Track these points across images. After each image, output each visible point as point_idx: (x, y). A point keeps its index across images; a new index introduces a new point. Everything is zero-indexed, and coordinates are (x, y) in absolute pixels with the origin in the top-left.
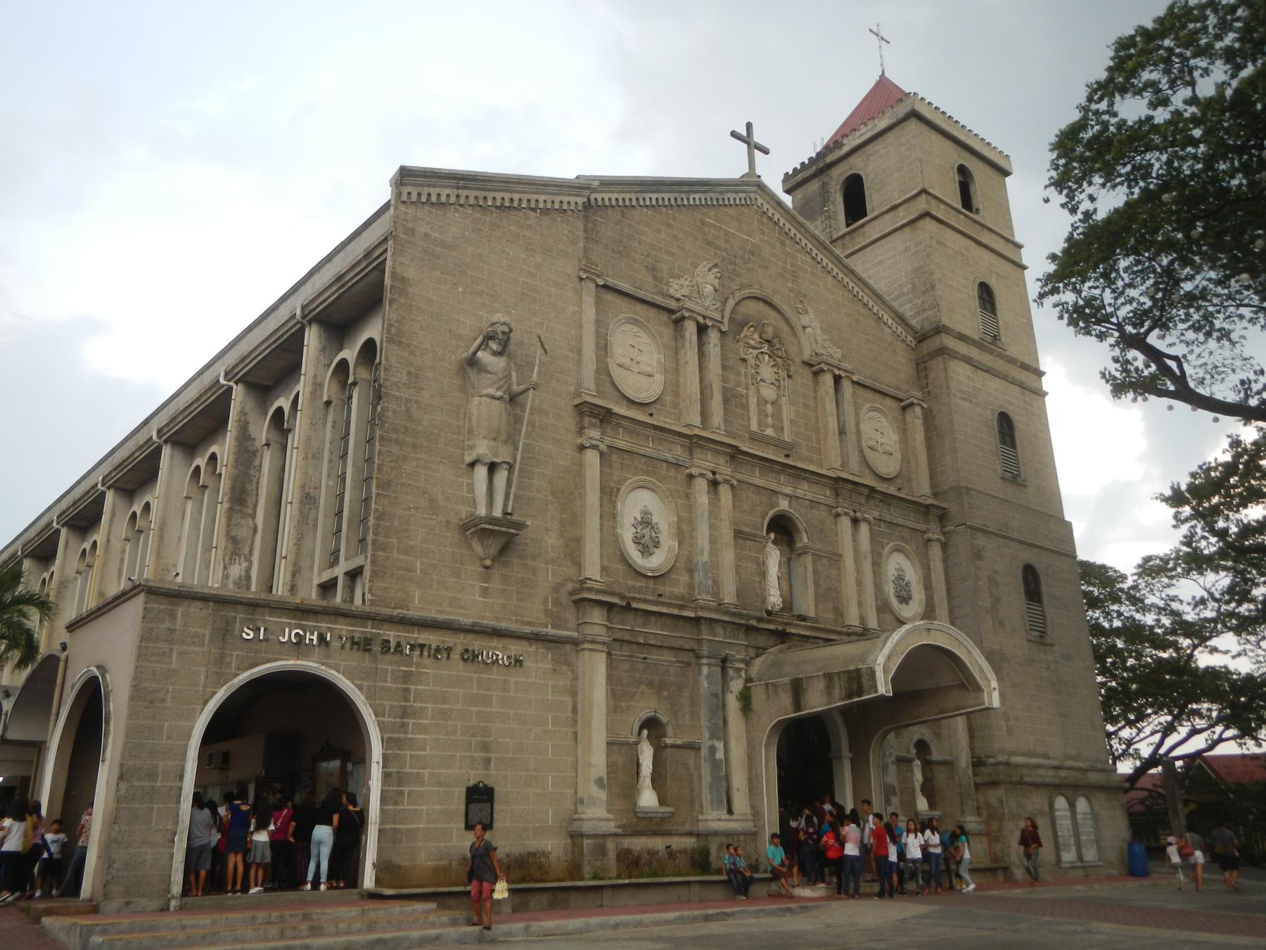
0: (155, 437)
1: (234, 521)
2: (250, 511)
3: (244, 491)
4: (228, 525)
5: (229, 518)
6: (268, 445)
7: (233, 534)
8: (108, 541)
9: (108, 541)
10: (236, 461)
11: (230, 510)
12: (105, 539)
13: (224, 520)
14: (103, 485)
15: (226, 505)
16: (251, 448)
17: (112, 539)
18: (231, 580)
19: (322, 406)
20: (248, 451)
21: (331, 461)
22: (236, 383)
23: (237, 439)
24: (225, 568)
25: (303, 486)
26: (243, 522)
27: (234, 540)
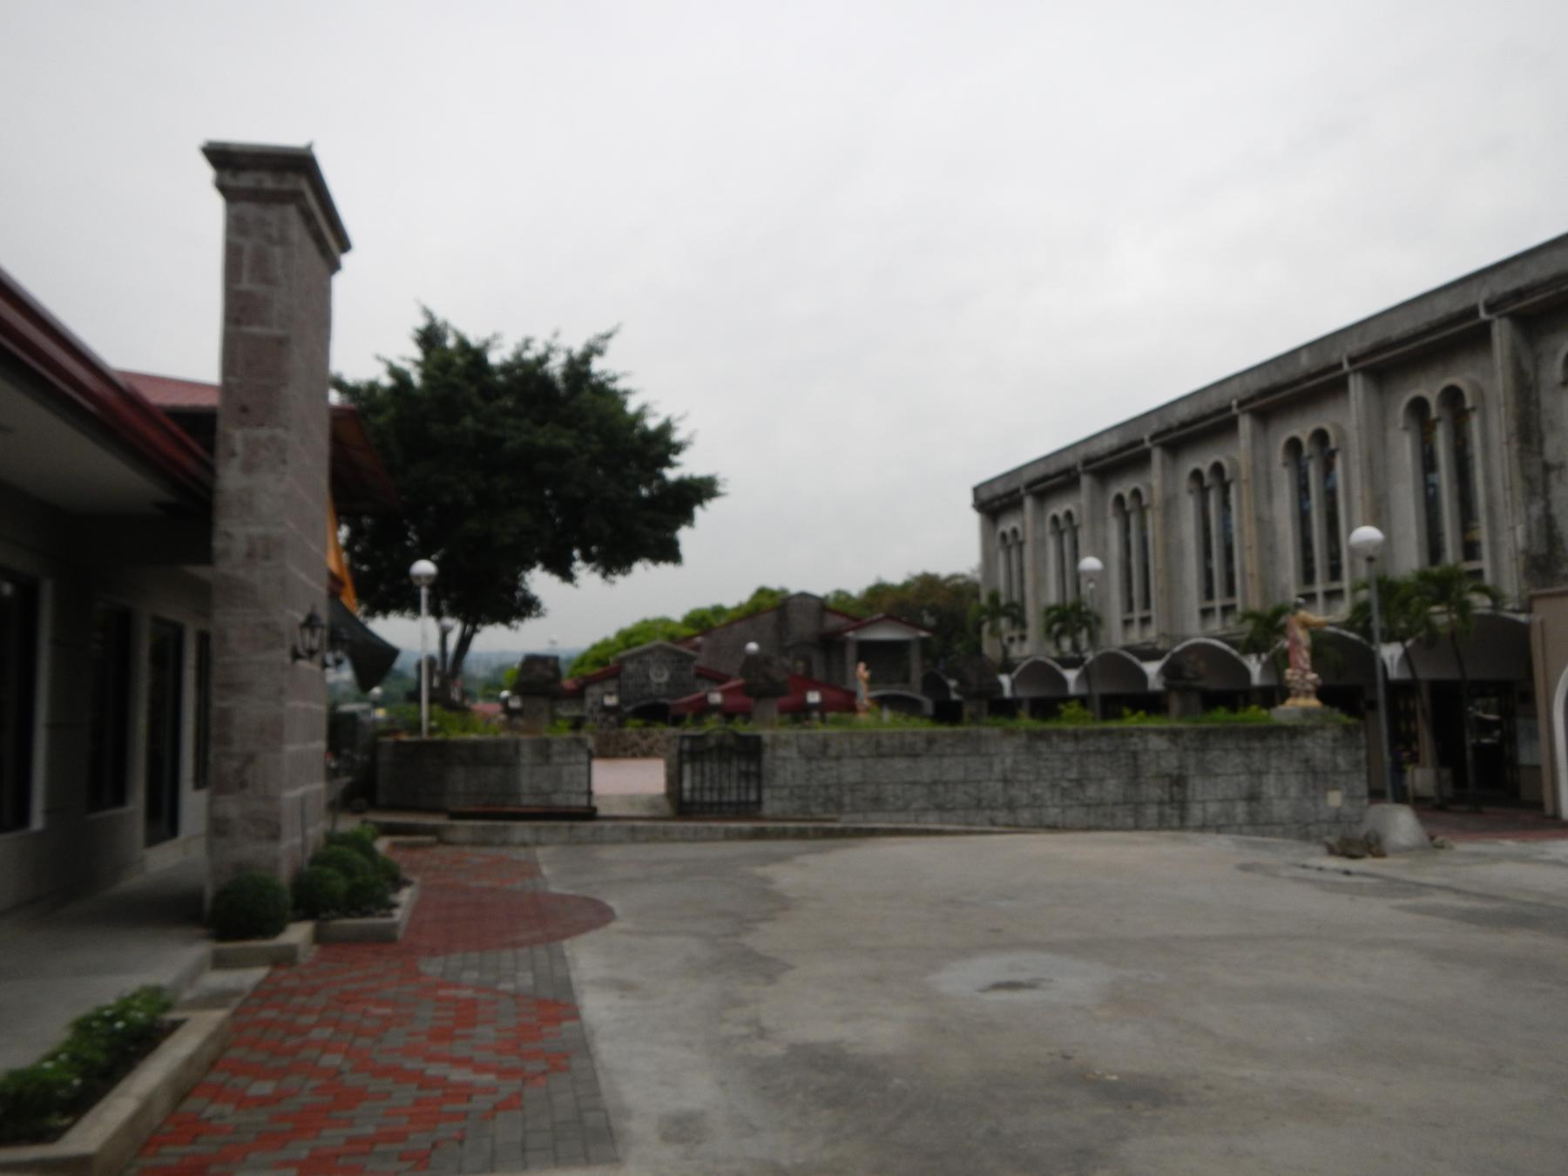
5: (1521, 458)
11: (1521, 450)
15: (1515, 446)
27: (1528, 480)
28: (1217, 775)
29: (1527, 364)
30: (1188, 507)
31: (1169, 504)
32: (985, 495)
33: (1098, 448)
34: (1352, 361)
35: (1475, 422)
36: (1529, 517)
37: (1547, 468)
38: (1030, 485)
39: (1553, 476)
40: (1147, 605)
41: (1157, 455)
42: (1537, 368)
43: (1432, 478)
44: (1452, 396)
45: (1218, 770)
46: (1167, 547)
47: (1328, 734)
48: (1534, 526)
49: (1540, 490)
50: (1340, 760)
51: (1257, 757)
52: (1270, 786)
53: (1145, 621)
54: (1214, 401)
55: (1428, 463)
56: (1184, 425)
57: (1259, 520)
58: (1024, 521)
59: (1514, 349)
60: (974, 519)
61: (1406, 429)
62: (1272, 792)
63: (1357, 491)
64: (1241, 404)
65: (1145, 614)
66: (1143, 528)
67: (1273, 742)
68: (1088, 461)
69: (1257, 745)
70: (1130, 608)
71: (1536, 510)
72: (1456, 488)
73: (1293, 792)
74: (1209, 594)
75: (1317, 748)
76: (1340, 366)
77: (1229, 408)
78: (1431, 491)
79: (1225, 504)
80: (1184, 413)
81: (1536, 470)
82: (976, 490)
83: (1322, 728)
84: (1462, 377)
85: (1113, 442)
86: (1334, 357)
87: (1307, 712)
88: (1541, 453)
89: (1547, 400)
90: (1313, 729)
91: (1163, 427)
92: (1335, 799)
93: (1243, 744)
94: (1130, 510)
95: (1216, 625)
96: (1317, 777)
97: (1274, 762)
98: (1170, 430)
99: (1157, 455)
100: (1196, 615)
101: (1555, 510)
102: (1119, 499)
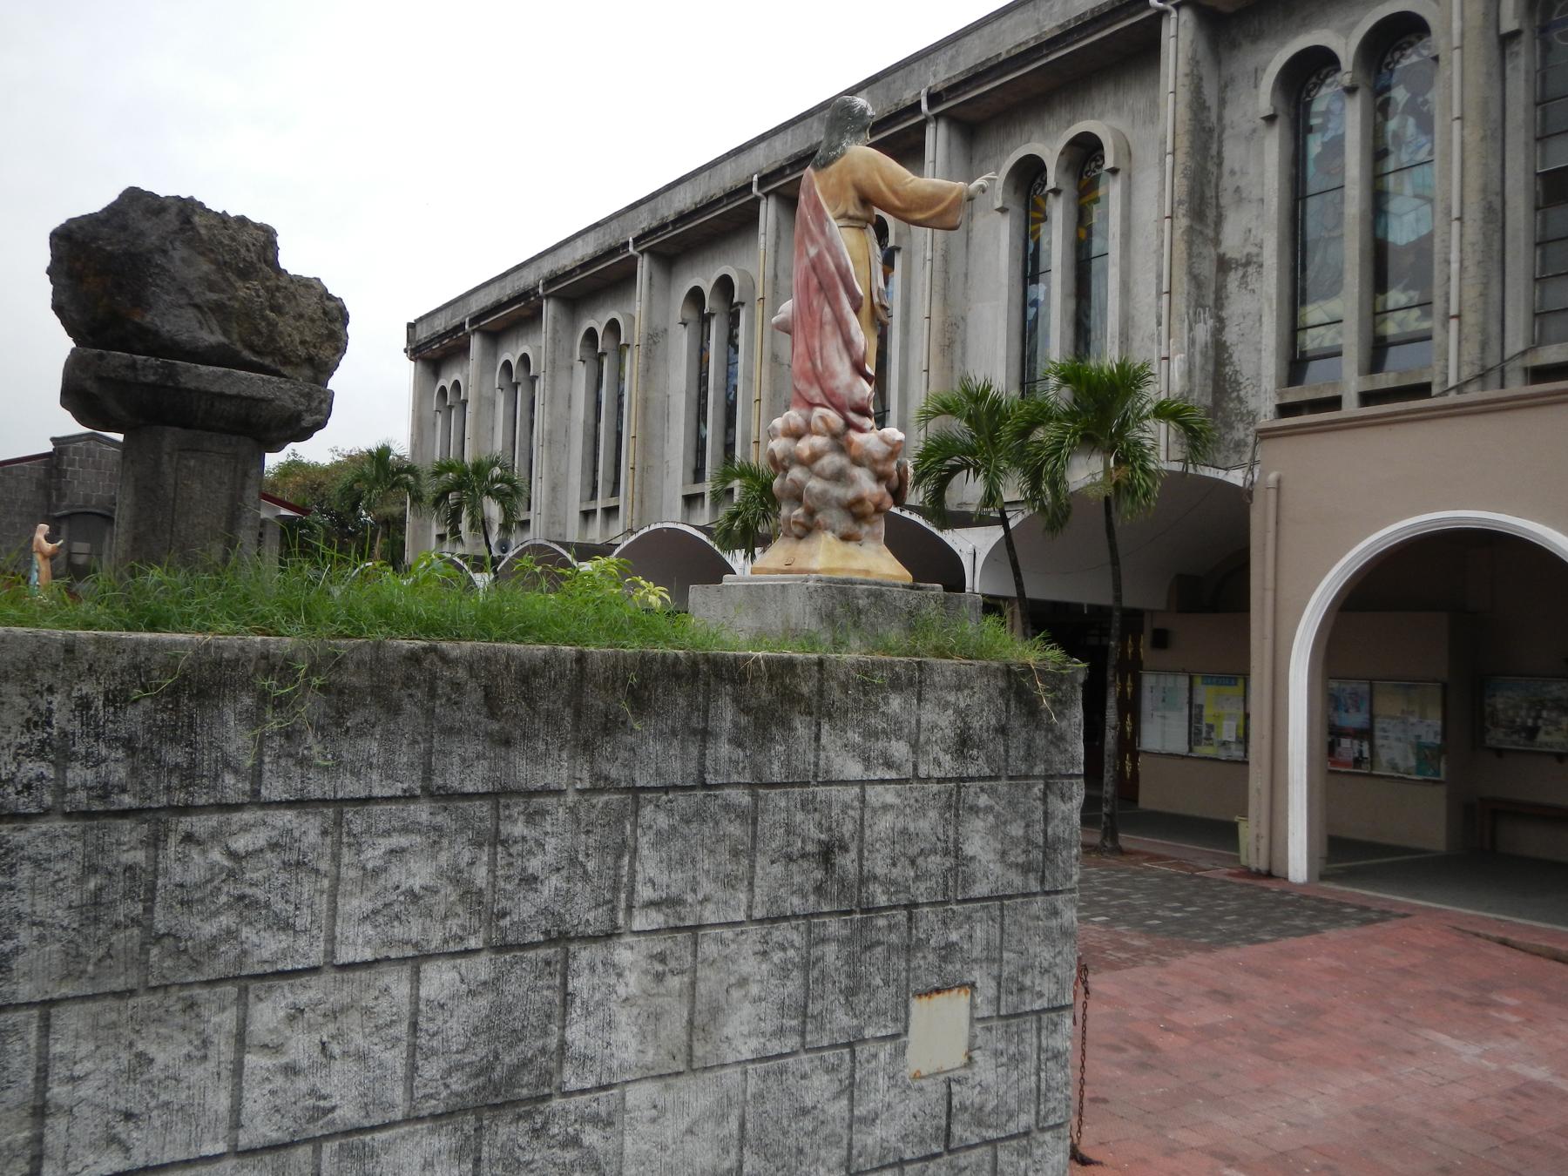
0: (924, 107)
1: (1195, 250)
2: (1210, 233)
3: (1202, 197)
4: (1190, 256)
5: (1190, 244)
6: (1270, 119)
7: (1196, 271)
8: (776, 276)
9: (776, 276)
10: (1192, 143)
11: (1190, 230)
12: (770, 273)
13: (1181, 247)
14: (760, 187)
15: (1183, 222)
16: (1207, 125)
17: (780, 274)
18: (1198, 348)
19: (1495, 40)
20: (1203, 129)
21: (1527, 144)
22: (1177, 7)
23: (1190, 106)
24: (1191, 329)
25: (1484, 190)
26: (1205, 251)
27: (1196, 280)
28: (250, 982)
29: (1210, 93)
30: (681, 343)
31: (655, 338)
32: (423, 334)
33: (568, 259)
34: (934, 99)
35: (1113, 190)
36: (1192, 342)
37: (1224, 265)
38: (476, 319)
39: (1233, 279)
40: (615, 491)
41: (644, 266)
42: (1222, 103)
43: (1038, 291)
44: (1085, 151)
45: (267, 946)
46: (645, 403)
47: (938, 719)
48: (1198, 359)
49: (1210, 300)
50: (978, 844)
51: (547, 843)
52: (617, 1012)
53: (610, 512)
54: (728, 178)
55: (1030, 269)
56: (683, 218)
57: (775, 358)
58: (469, 373)
59: (1194, 62)
60: (406, 371)
61: (1003, 210)
62: (627, 1045)
63: (921, 308)
64: (764, 180)
65: (612, 503)
66: (619, 379)
67: (654, 755)
68: (551, 281)
69: (560, 770)
70: (593, 496)
71: (1203, 332)
72: (1072, 305)
73: (742, 1031)
74: (698, 474)
75: (875, 785)
76: (916, 106)
77: (748, 187)
78: (1031, 312)
79: (732, 341)
80: (684, 200)
81: (1207, 269)
82: (411, 326)
83: (914, 682)
84: (1102, 121)
85: (585, 250)
86: (908, 97)
87: (844, 601)
88: (1217, 242)
89: (1234, 153)
90: (866, 684)
91: (655, 224)
92: (940, 1030)
93: (467, 771)
94: (603, 351)
95: (704, 516)
96: (862, 925)
97: (652, 871)
98: (663, 226)
99: (644, 266)
100: (679, 502)
101: (1230, 336)
102: (591, 335)
